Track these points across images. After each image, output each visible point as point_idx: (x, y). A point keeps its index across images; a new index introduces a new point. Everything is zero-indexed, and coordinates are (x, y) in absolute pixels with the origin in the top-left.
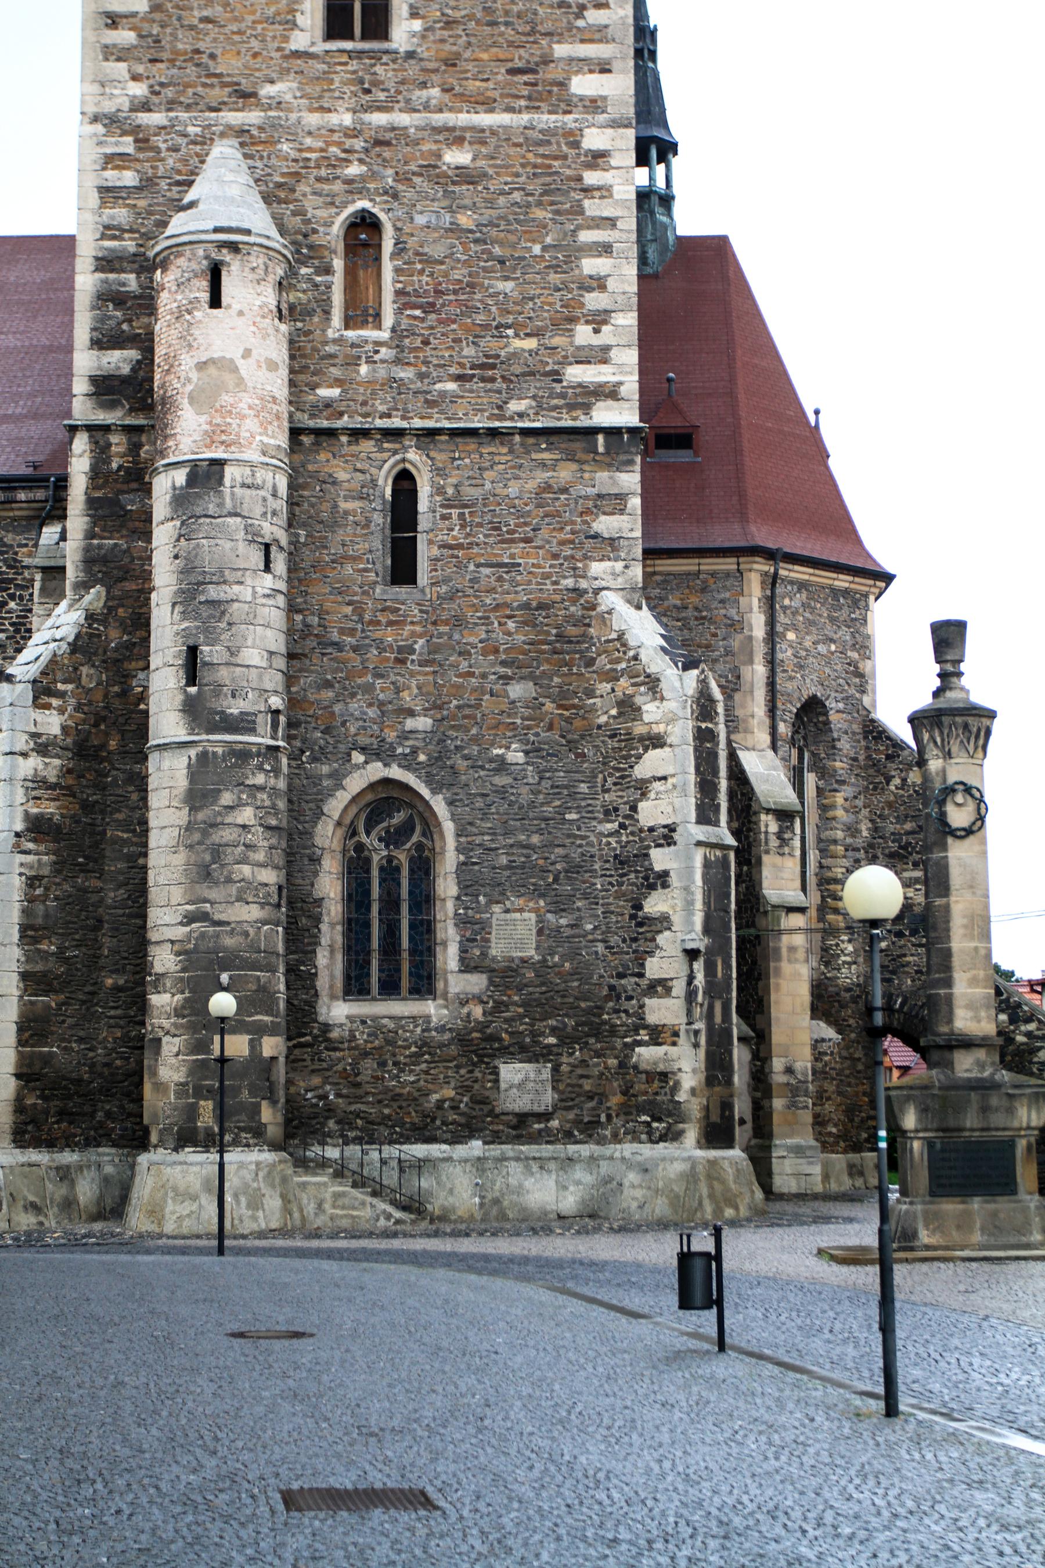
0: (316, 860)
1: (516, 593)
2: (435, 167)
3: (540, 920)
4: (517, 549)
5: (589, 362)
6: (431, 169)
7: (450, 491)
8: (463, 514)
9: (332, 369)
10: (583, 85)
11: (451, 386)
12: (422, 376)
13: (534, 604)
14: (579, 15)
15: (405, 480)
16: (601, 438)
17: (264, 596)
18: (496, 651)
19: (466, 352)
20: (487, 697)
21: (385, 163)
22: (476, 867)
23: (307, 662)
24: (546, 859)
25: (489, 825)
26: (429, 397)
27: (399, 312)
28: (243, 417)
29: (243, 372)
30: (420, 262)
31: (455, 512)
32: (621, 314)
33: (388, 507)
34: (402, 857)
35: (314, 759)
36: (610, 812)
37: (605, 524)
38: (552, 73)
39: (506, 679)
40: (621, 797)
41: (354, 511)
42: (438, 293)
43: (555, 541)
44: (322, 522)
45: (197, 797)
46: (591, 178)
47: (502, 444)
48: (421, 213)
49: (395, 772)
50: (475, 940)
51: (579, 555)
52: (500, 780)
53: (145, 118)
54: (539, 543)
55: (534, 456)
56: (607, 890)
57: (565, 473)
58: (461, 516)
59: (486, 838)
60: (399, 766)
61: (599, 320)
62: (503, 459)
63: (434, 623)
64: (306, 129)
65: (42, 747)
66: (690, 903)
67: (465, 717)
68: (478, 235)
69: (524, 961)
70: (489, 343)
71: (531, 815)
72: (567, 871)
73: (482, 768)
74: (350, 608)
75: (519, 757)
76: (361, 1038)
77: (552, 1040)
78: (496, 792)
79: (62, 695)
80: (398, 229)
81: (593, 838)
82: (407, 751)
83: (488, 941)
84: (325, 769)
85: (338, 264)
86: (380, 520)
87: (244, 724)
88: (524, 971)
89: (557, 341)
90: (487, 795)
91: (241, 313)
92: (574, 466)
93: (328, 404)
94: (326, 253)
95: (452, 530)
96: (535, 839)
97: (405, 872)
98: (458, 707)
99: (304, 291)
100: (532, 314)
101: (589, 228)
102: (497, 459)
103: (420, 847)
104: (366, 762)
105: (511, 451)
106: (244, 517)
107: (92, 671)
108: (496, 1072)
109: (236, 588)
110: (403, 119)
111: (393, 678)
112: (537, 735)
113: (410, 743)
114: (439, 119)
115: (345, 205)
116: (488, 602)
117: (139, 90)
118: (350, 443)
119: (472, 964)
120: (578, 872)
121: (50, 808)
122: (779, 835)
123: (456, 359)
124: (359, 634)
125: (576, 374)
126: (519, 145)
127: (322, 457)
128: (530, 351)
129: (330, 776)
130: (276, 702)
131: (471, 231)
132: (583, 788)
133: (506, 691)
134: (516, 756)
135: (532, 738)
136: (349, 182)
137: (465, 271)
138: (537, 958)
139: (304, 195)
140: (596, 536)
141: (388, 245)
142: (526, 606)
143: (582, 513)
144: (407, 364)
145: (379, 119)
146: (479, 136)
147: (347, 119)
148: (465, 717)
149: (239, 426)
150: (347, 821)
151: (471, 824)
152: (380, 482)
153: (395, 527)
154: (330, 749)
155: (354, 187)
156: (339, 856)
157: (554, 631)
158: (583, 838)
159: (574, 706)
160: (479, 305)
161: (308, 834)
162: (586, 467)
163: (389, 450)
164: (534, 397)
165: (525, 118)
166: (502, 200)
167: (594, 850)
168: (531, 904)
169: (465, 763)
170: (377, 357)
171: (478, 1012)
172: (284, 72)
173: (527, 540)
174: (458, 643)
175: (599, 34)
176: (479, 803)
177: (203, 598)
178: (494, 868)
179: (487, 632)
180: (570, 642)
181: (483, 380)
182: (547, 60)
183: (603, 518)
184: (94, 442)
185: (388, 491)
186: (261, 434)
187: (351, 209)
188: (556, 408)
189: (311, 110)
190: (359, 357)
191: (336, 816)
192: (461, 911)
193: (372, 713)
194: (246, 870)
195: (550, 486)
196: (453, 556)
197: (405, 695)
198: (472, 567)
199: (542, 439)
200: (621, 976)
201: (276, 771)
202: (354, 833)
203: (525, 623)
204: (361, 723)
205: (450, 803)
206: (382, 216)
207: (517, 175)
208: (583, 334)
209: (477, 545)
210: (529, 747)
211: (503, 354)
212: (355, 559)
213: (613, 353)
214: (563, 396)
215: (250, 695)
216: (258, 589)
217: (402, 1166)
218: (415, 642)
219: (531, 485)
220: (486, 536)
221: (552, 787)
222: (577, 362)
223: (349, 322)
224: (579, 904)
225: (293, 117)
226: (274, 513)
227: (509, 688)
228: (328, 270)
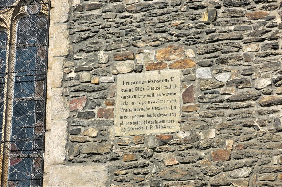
3: (188, 79)
22: (96, 12)
50: (91, 114)
69: (164, 141)
83: (109, 114)
88: (163, 155)
119: (86, 149)
138: (182, 135)
168: (174, 57)
192: (73, 75)
224: (248, 49)
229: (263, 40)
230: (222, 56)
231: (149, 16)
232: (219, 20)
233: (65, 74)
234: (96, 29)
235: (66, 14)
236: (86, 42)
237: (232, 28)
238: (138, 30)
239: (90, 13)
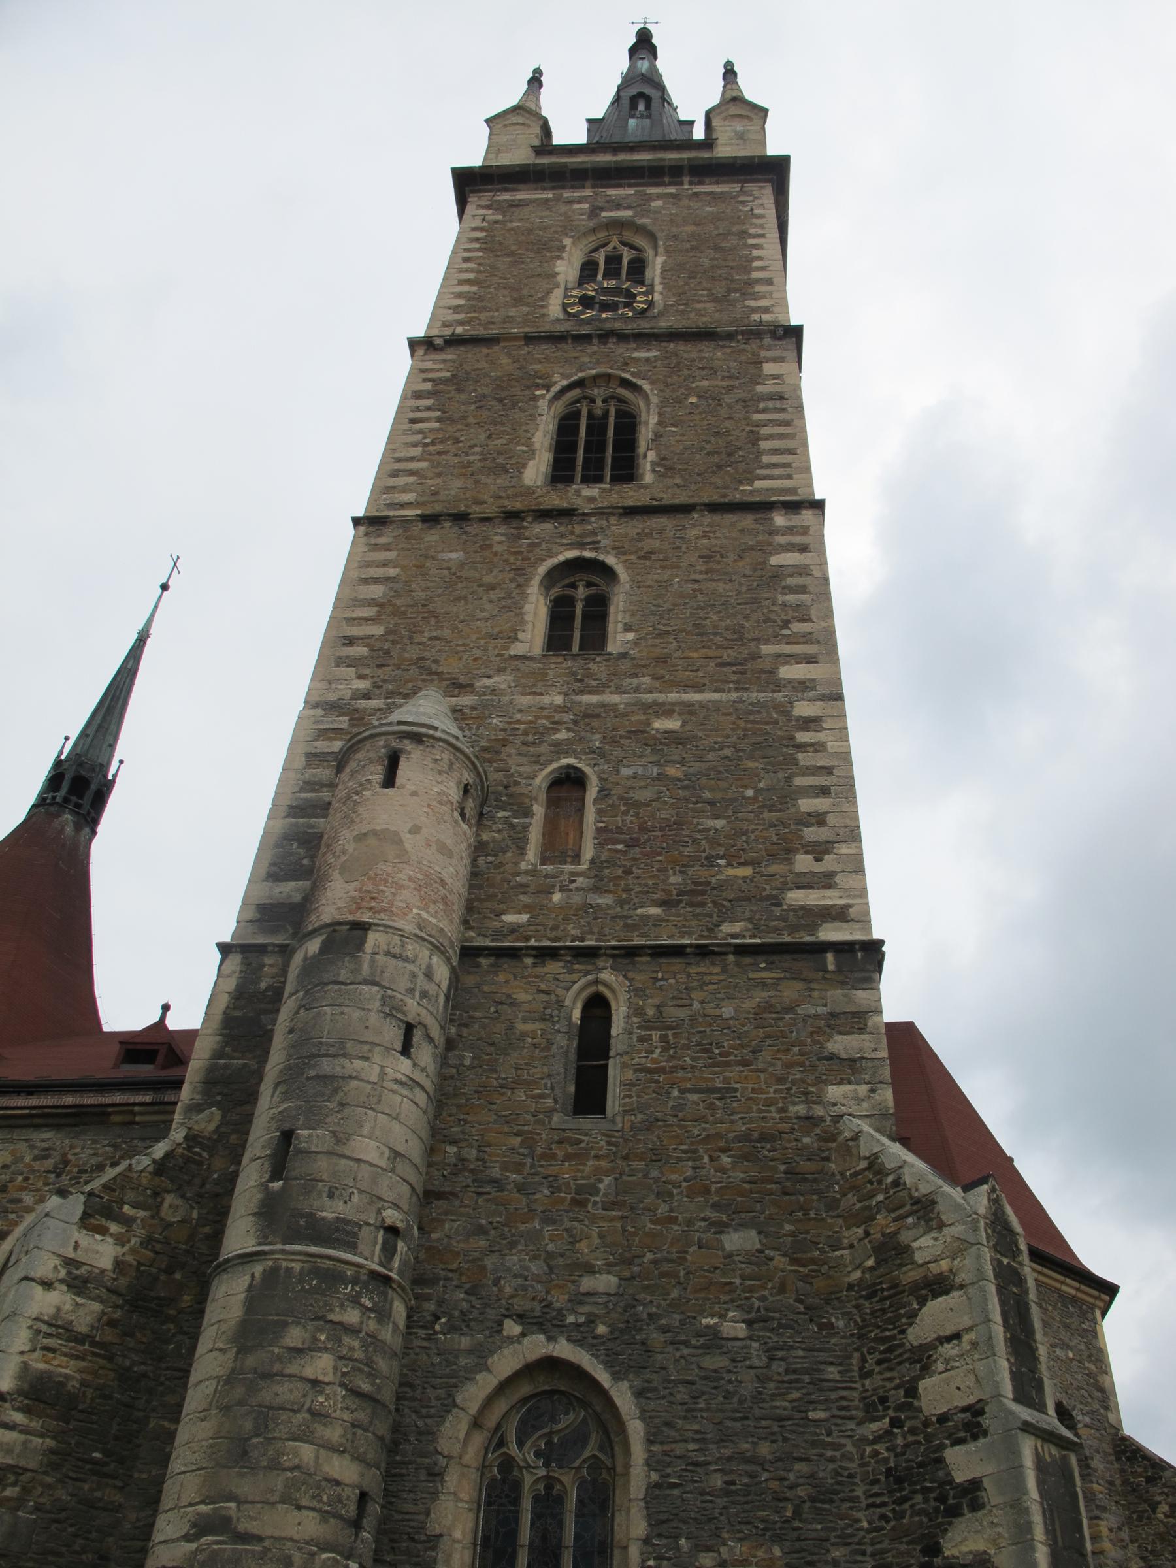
0: (436, 1474)
1: (732, 1122)
2: (643, 732)
4: (733, 1073)
5: (812, 888)
6: (639, 732)
7: (651, 1012)
8: (666, 1036)
9: (521, 897)
11: (655, 911)
12: (621, 903)
13: (756, 1135)
14: (786, 624)
15: (597, 1006)
16: (830, 957)
17: (396, 1081)
18: (706, 1191)
19: (673, 880)
20: (694, 1248)
21: (593, 730)
22: (676, 1492)
23: (457, 1203)
24: (783, 1479)
25: (696, 1427)
26: (629, 921)
28: (400, 887)
29: (407, 846)
30: (624, 805)
31: (655, 1035)
32: (844, 845)
33: (575, 1031)
35: (452, 1329)
37: (841, 1044)
38: (759, 664)
39: (720, 1227)
40: (890, 1379)
41: (534, 1032)
42: (643, 829)
43: (779, 1063)
44: (493, 1044)
45: (252, 1332)
46: (803, 737)
47: (713, 964)
48: (629, 766)
49: (563, 1349)
51: (811, 1078)
53: (363, 704)
54: (761, 1066)
55: (751, 975)
56: (878, 1529)
57: (790, 991)
58: (664, 1038)
59: (691, 1446)
60: (569, 1340)
62: (715, 979)
63: (626, 1158)
64: (517, 707)
65: (78, 1280)
66: (1023, 1530)
67: (663, 1275)
68: (687, 782)
70: (699, 872)
71: (757, 1412)
72: (813, 1500)
73: (686, 1344)
74: (519, 1139)
75: (740, 1330)
78: (705, 1378)
79: (127, 1221)
80: (601, 779)
81: (850, 1448)
82: (582, 1319)
84: (465, 1342)
85: (539, 810)
86: (565, 1044)
87: (342, 1234)
89: (773, 869)
90: (693, 1383)
91: (414, 794)
92: (800, 985)
93: (514, 929)
94: (527, 801)
95: (652, 1052)
96: (765, 1449)
97: (571, 1503)
98: (654, 1262)
99: (499, 831)
100: (745, 846)
101: (803, 775)
102: (707, 978)
103: (595, 1464)
104: (523, 1335)
105: (724, 971)
106: (384, 987)
107: (179, 1202)
109: (358, 1064)
110: (616, 699)
111: (567, 1224)
112: (763, 1299)
113: (586, 1309)
114: (648, 698)
115: (550, 762)
116: (696, 1132)
117: (362, 685)
118: (535, 965)
120: (831, 1501)
123: (661, 886)
124: (527, 1170)
125: (796, 897)
126: (730, 714)
127: (501, 978)
128: (744, 878)
129: (470, 1352)
130: (392, 1216)
131: (679, 780)
132: (832, 1372)
133: (720, 1241)
134: (734, 1328)
135: (757, 1304)
137: (673, 812)
139: (510, 755)
140: (832, 1057)
141: (592, 792)
142: (746, 1137)
143: (812, 1033)
144: (606, 891)
146: (689, 709)
147: (559, 700)
148: (663, 1275)
149: (394, 894)
150: (492, 1420)
151: (667, 1424)
152: (567, 1003)
153: (584, 1052)
154: (475, 1314)
155: (560, 749)
156: (474, 1475)
157: (782, 1168)
158: (837, 1447)
159: (813, 1261)
160: (686, 839)
161: (429, 1434)
162: (814, 986)
163: (579, 971)
164: (750, 920)
165: (734, 695)
166: (711, 756)
167: (853, 1466)
169: (662, 1338)
170: (572, 886)
172: (500, 670)
173: (745, 1063)
174: (656, 1181)
176: (682, 1394)
177: (312, 1073)
178: (703, 1493)
179: (694, 1168)
180: (805, 1180)
181: (691, 904)
182: (754, 656)
183: (839, 1038)
184: (246, 963)
185: (577, 1015)
186: (419, 908)
187: (555, 765)
188: (776, 929)
189: (524, 694)
190: (553, 886)
191: (473, 1408)
192: (651, 1563)
193: (535, 1268)
194: (307, 1452)
195: (772, 1006)
196: (652, 1081)
197: (583, 1246)
198: (675, 1093)
199: (760, 958)
202: (501, 1443)
203: (745, 1157)
204: (520, 1281)
205: (639, 1394)
206: (587, 770)
207: (728, 737)
208: (804, 862)
209: (683, 1068)
210: (752, 1315)
211: (713, 881)
212: (528, 1084)
213: (838, 879)
214: (783, 919)
215: (355, 1198)
216: (389, 1071)
218: (600, 1181)
219: (748, 1005)
220: (693, 1059)
221: (787, 1371)
222: (798, 888)
224: (837, 1553)
225: (506, 699)
226: (424, 994)
227: (724, 1237)
228: (528, 813)
229: (850, 1544)
230: (809, 1558)
231: (733, 1503)
232: (804, 1516)
233: (644, 1561)
234: (675, 1511)
235: (643, 1490)
236: (665, 1526)
237: (819, 1527)
238: (722, 1518)
239: (668, 1492)
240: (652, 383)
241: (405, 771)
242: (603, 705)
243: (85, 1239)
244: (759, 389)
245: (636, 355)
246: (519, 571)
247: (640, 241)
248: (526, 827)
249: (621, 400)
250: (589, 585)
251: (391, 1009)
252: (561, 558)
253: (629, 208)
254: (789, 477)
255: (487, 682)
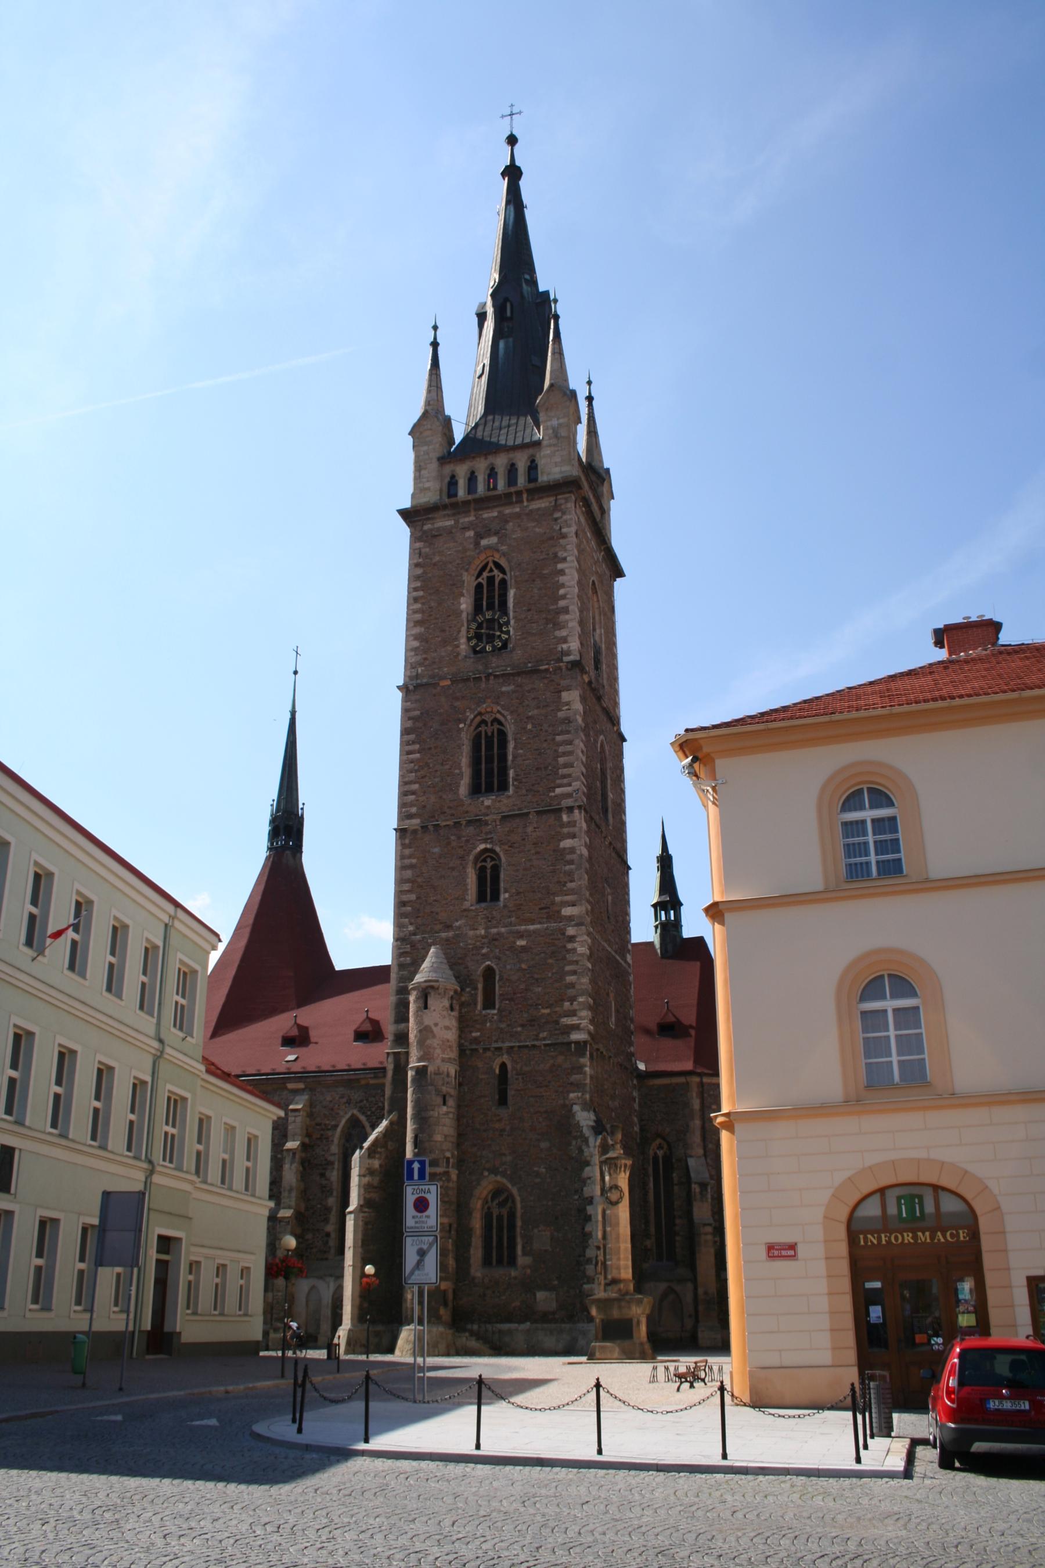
0: (470, 1214)
6: (512, 948)
10: (567, 911)
11: (519, 1029)
14: (564, 885)
15: (503, 1066)
27: (501, 1002)
28: (435, 1048)
34: (505, 1212)
36: (576, 1192)
37: (575, 1077)
46: (569, 946)
52: (538, 1180)
57: (560, 1059)
61: (572, 1000)
76: (486, 1281)
77: (556, 1282)
79: (380, 1153)
85: (480, 986)
89: (557, 1009)
92: (563, 1057)
93: (476, 1038)
96: (550, 1203)
97: (505, 1217)
103: (511, 1208)
108: (535, 1295)
110: (503, 930)
117: (411, 928)
121: (374, 1196)
122: (701, 1193)
130: (448, 1154)
136: (483, 955)
140: (572, 1084)
142: (546, 1112)
145: (494, 931)
155: (486, 957)
171: (529, 1271)
175: (572, 892)
182: (553, 903)
185: (497, 1071)
200: (580, 1256)
201: (449, 1180)
205: (519, 1190)
208: (567, 1004)
217: (500, 1331)
223: (485, 1008)
228: (476, 989)
240: (512, 713)
241: (430, 1002)
242: (498, 934)
243: (370, 1161)
244: (560, 714)
245: (504, 689)
246: (462, 858)
247: (503, 562)
248: (476, 994)
249: (500, 723)
250: (493, 859)
251: (438, 1092)
252: (478, 849)
253: (496, 533)
254: (570, 785)
255: (457, 924)
